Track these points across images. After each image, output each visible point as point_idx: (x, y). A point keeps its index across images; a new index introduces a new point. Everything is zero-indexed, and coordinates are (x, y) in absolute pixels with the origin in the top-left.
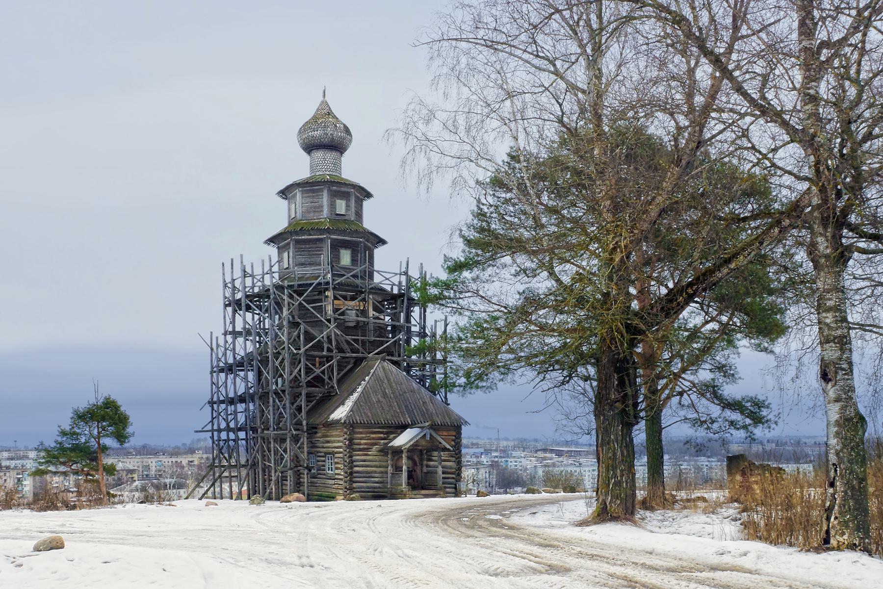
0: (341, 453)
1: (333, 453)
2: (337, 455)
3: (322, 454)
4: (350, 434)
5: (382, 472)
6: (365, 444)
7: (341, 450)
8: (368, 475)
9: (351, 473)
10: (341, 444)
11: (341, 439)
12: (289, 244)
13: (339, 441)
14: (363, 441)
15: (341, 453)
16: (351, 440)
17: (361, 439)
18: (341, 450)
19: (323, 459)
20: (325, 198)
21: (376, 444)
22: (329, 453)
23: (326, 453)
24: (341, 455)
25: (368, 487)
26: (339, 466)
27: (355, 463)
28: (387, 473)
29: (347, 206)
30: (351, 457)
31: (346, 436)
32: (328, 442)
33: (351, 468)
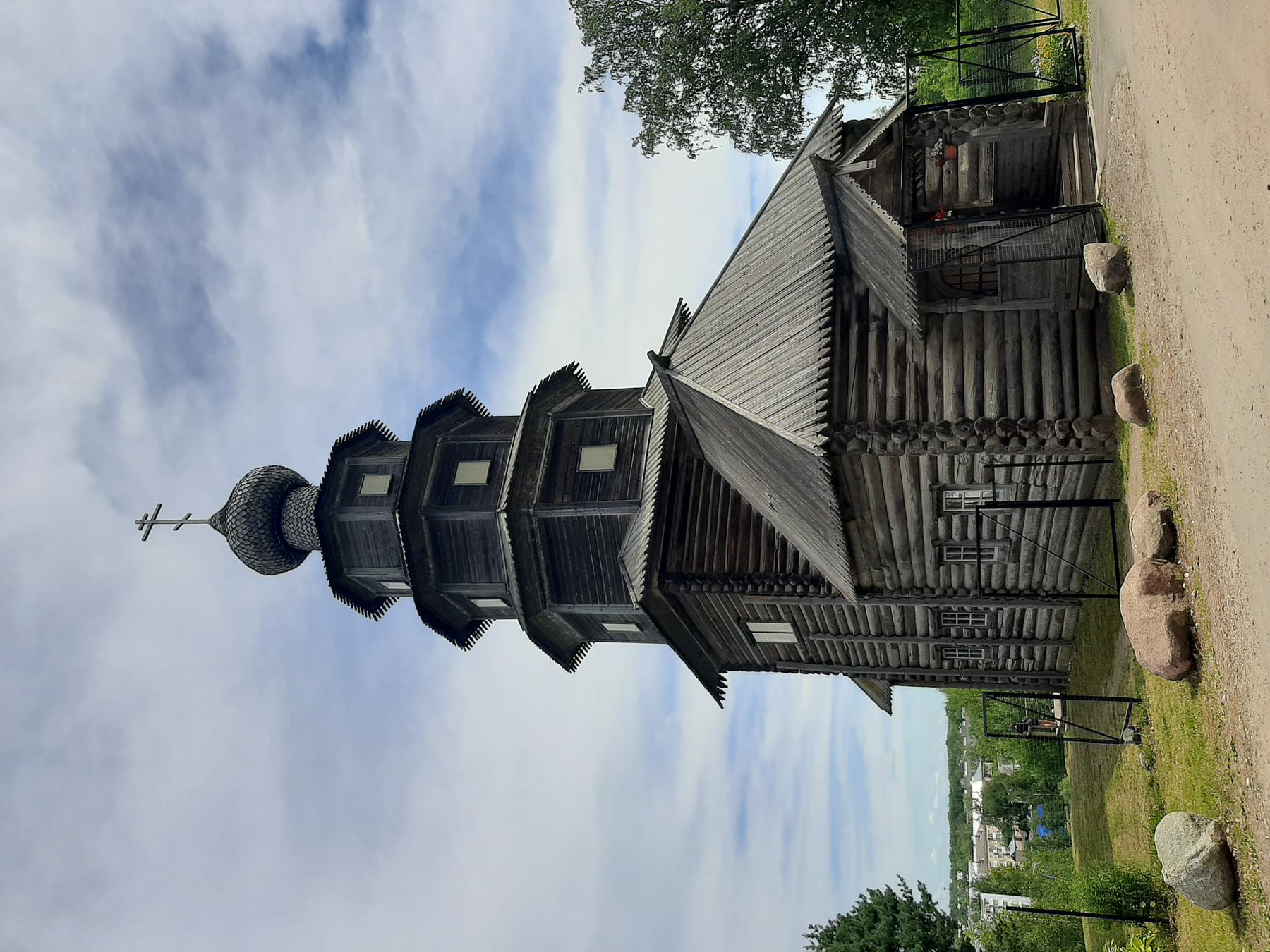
0: (933, 460)
1: (938, 489)
2: (943, 477)
3: (941, 524)
4: (865, 429)
5: (1000, 331)
6: (901, 383)
7: (924, 460)
8: (1010, 373)
9: (1008, 425)
10: (903, 461)
11: (884, 461)
12: (452, 596)
13: (895, 470)
14: (892, 392)
15: (933, 460)
16: (886, 429)
17: (882, 398)
18: (924, 460)
19: (956, 520)
20: (356, 516)
21: (901, 352)
22: (937, 502)
23: (938, 512)
24: (942, 461)
25: (1059, 371)
26: (979, 471)
27: (971, 414)
28: (1000, 316)
29: (378, 471)
30: (946, 428)
31: (874, 444)
32: (901, 506)
33: (988, 425)
